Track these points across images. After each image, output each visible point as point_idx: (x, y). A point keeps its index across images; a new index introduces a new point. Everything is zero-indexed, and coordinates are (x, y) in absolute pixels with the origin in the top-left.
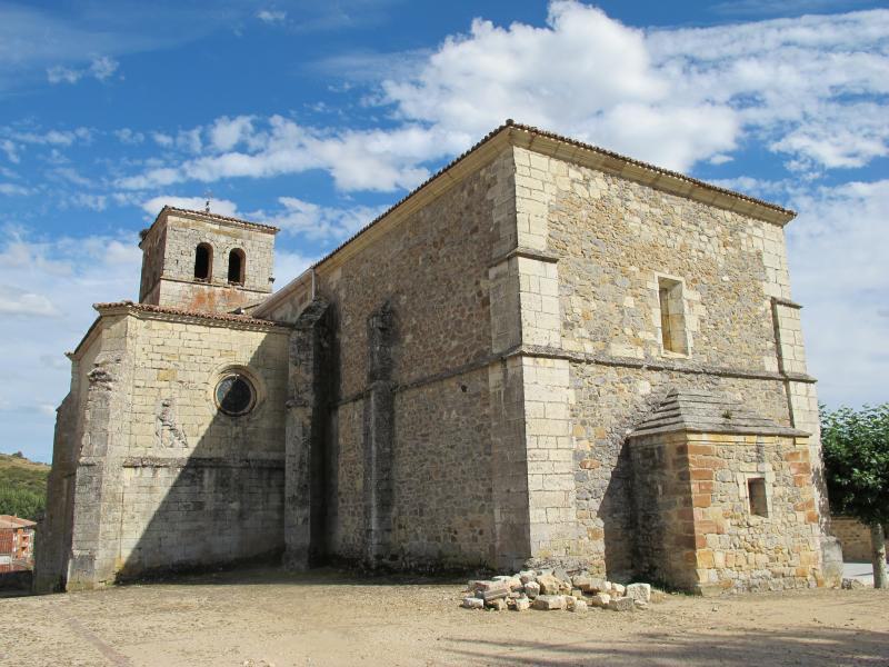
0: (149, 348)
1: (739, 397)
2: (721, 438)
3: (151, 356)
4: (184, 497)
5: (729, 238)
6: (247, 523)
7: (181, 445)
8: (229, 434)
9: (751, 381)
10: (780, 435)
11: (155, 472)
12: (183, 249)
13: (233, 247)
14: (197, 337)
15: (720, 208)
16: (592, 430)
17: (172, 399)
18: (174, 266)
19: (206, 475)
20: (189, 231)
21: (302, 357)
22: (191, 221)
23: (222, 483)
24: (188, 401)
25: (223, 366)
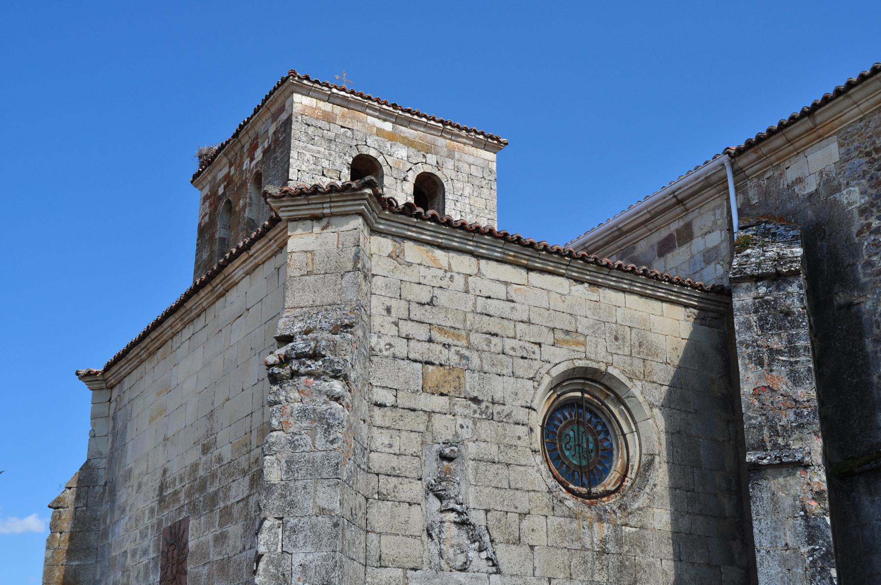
3: (407, 328)
7: (484, 566)
8: (587, 541)
12: (325, 164)
13: (421, 169)
14: (500, 291)
17: (457, 442)
20: (336, 129)
21: (776, 343)
22: (338, 110)
25: (562, 368)
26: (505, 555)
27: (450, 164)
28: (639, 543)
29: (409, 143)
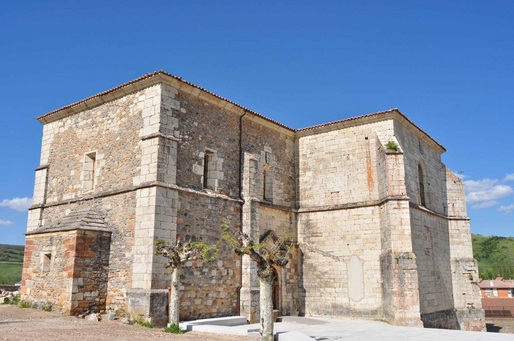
2: (36, 236)
9: (117, 196)
10: (61, 231)
15: (120, 98)
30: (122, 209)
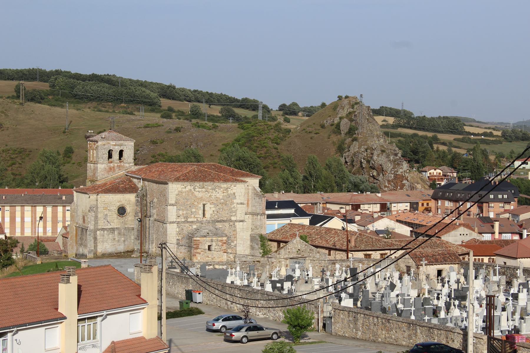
0: (101, 202)
1: (221, 226)
3: (102, 204)
4: (111, 237)
5: (225, 191)
6: (126, 243)
11: (104, 231)
12: (104, 153)
16: (182, 235)
18: (101, 159)
19: (116, 232)
23: (119, 234)
24: (111, 214)
26: (111, 224)
27: (125, 147)
28: (127, 221)
29: (118, 145)
30: (228, 228)
